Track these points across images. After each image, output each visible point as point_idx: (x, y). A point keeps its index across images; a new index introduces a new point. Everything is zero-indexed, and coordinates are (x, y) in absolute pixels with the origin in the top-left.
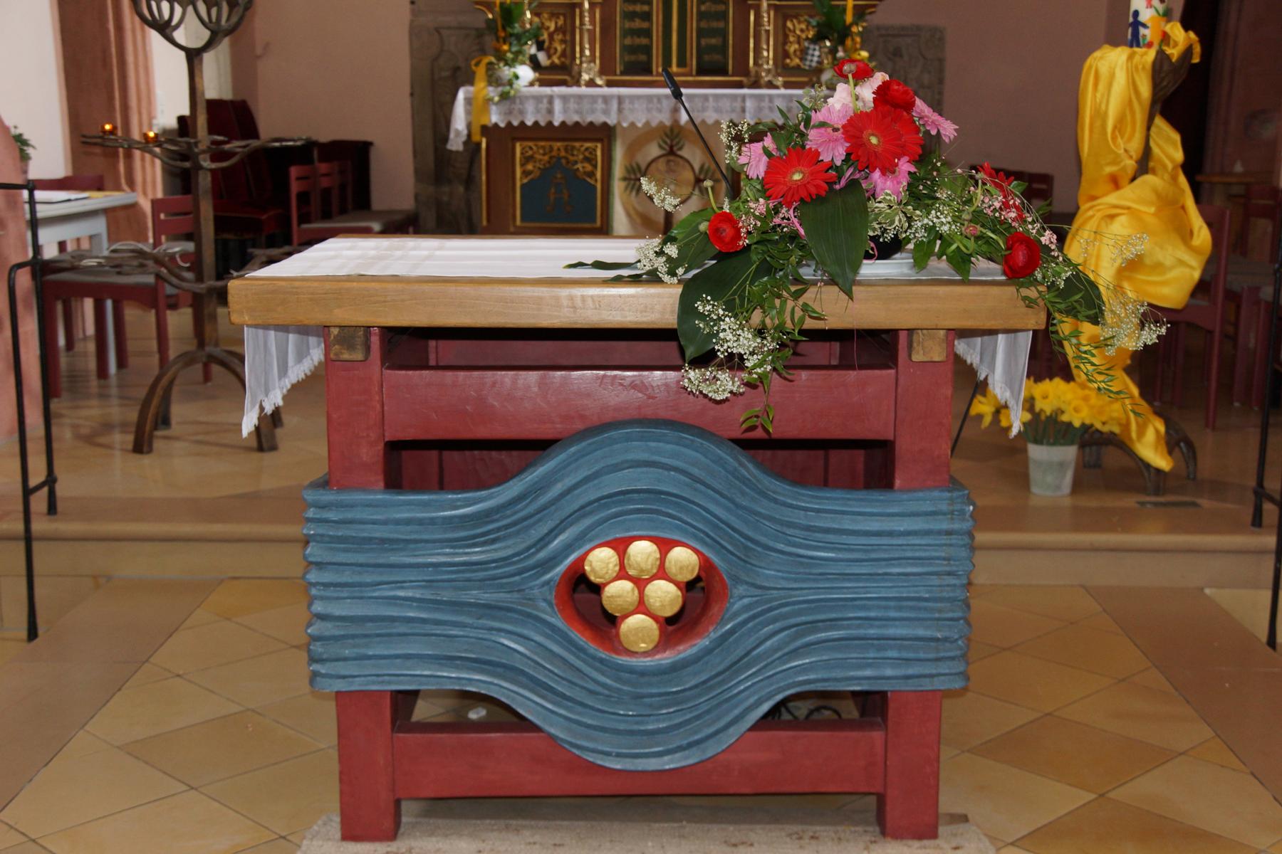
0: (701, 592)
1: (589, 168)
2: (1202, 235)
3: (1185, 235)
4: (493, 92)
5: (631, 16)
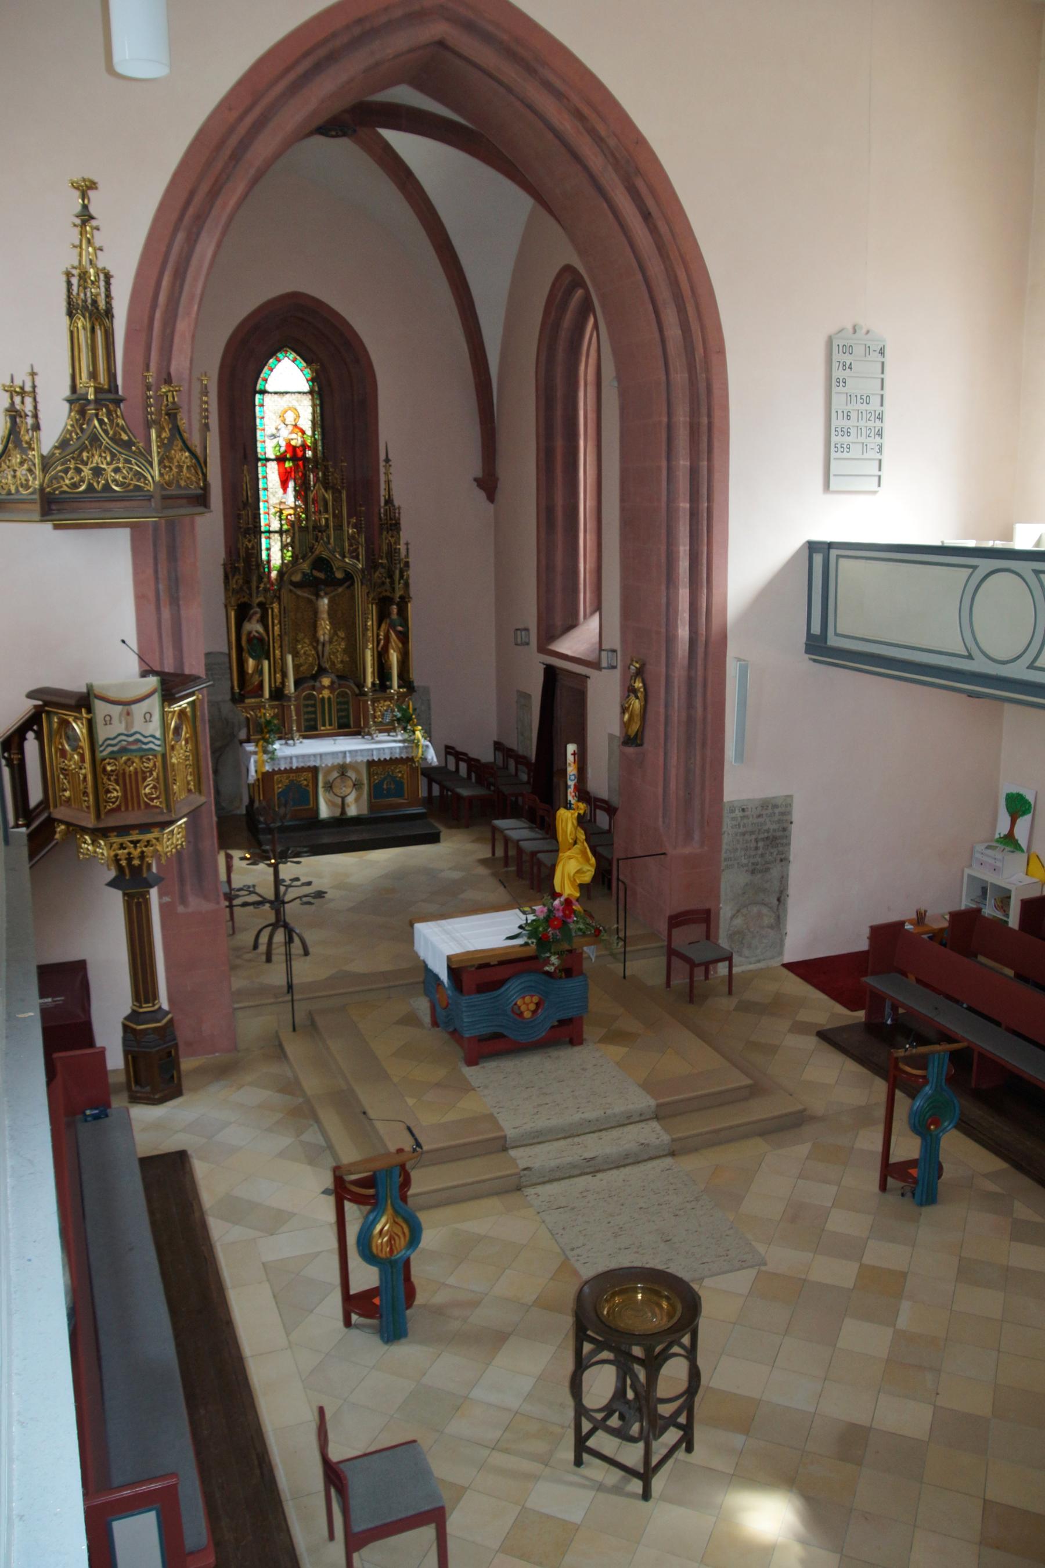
0: (538, 1005)
1: (305, 783)
2: (593, 860)
3: (588, 860)
4: (265, 757)
5: (307, 706)
